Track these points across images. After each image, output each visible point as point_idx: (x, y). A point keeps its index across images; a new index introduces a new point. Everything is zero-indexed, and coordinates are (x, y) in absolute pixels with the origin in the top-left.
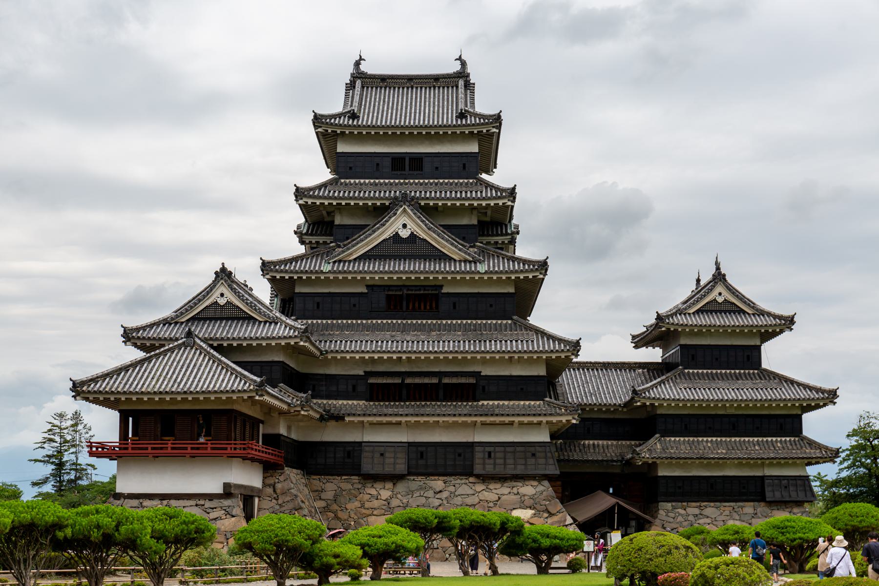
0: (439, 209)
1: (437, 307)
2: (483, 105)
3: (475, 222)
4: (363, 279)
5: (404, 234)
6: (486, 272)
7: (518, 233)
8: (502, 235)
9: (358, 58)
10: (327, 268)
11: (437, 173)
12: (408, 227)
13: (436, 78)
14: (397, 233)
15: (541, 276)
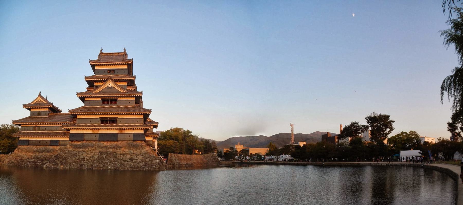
5: (110, 86)
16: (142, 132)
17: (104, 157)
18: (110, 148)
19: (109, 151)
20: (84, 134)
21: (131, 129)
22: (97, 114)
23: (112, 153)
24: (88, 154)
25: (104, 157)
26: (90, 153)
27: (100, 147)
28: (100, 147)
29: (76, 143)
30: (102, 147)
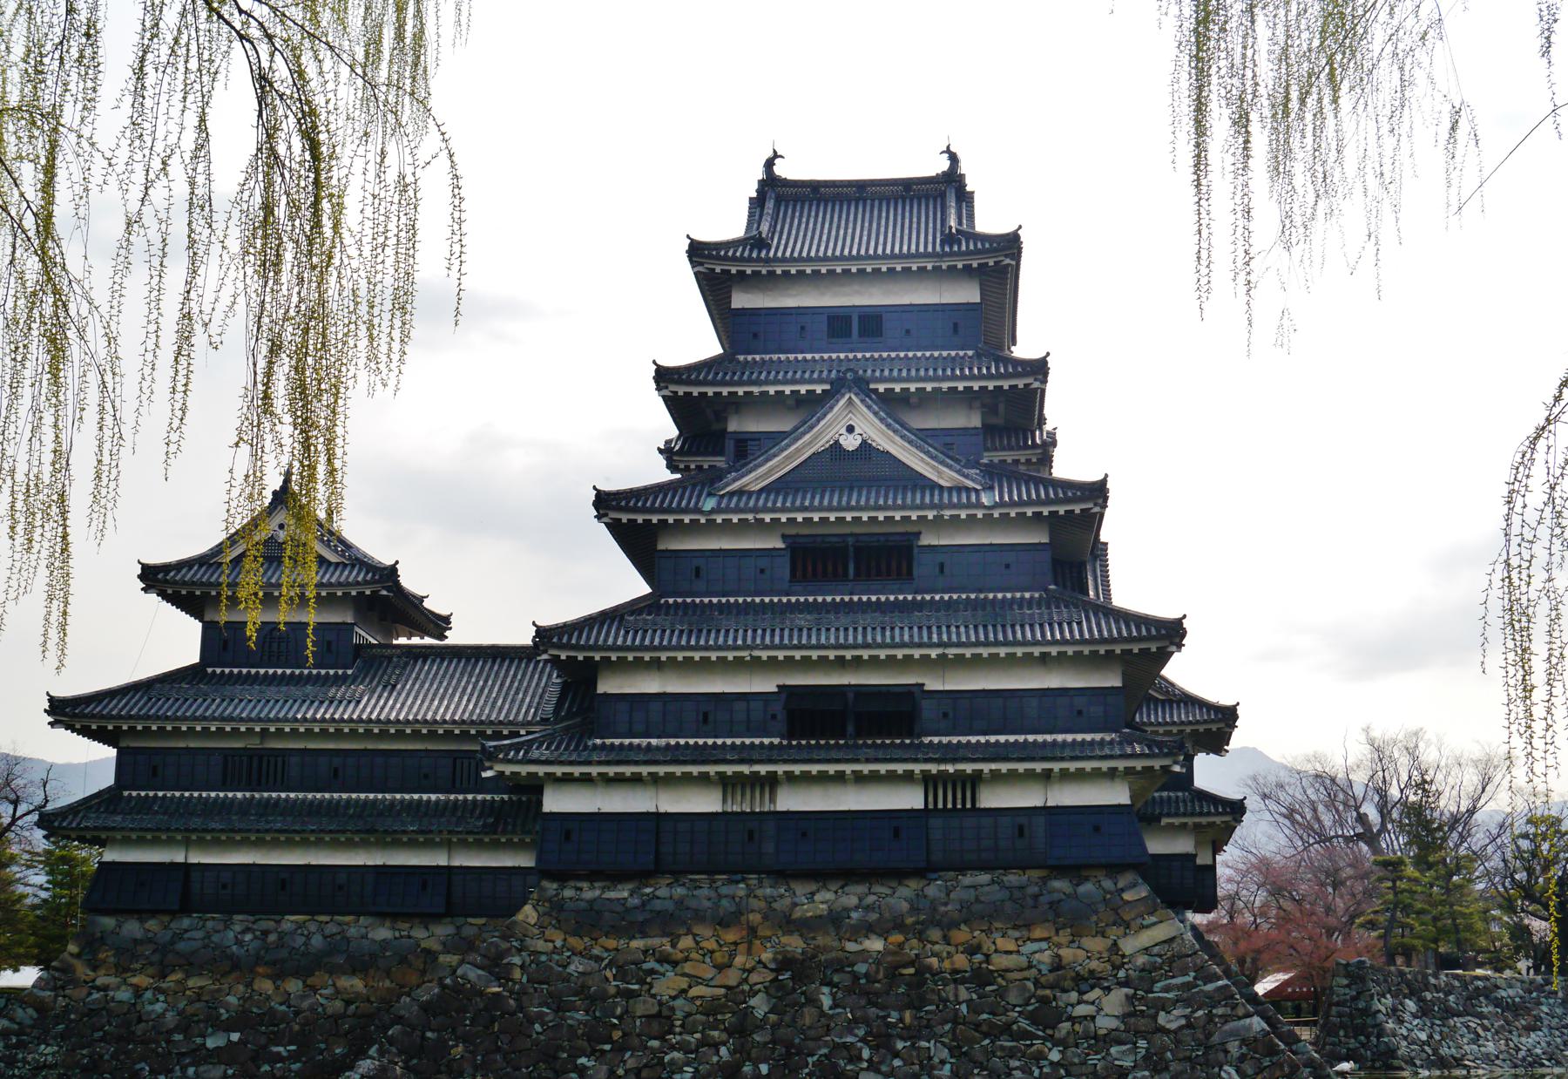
0: (913, 400)
1: (910, 573)
2: (989, 220)
3: (975, 421)
4: (776, 521)
5: (850, 443)
6: (995, 506)
7: (1054, 444)
8: (1026, 447)
9: (771, 154)
10: (709, 504)
11: (909, 339)
12: (858, 430)
13: (907, 184)
14: (837, 442)
15: (1097, 509)
16: (1118, 795)
17: (826, 1001)
18: (869, 929)
19: (864, 955)
20: (658, 817)
21: (1030, 775)
22: (756, 665)
23: (892, 967)
24: (696, 980)
25: (826, 1001)
26: (709, 973)
27: (789, 924)
28: (789, 924)
29: (590, 893)
30: (804, 927)
